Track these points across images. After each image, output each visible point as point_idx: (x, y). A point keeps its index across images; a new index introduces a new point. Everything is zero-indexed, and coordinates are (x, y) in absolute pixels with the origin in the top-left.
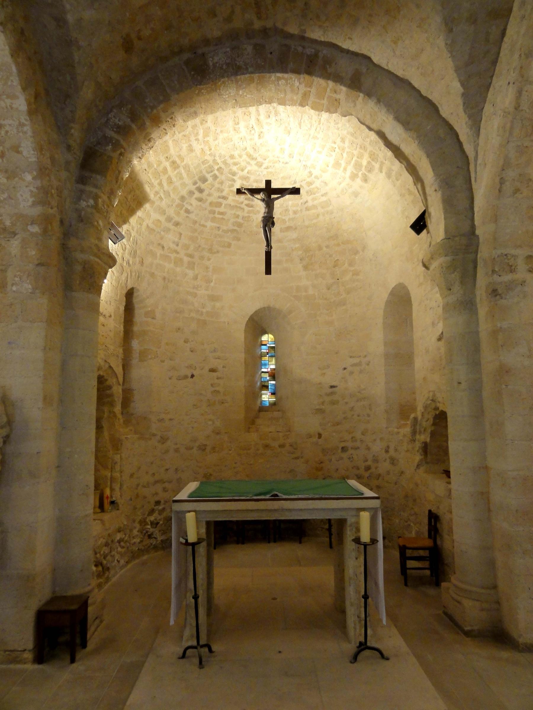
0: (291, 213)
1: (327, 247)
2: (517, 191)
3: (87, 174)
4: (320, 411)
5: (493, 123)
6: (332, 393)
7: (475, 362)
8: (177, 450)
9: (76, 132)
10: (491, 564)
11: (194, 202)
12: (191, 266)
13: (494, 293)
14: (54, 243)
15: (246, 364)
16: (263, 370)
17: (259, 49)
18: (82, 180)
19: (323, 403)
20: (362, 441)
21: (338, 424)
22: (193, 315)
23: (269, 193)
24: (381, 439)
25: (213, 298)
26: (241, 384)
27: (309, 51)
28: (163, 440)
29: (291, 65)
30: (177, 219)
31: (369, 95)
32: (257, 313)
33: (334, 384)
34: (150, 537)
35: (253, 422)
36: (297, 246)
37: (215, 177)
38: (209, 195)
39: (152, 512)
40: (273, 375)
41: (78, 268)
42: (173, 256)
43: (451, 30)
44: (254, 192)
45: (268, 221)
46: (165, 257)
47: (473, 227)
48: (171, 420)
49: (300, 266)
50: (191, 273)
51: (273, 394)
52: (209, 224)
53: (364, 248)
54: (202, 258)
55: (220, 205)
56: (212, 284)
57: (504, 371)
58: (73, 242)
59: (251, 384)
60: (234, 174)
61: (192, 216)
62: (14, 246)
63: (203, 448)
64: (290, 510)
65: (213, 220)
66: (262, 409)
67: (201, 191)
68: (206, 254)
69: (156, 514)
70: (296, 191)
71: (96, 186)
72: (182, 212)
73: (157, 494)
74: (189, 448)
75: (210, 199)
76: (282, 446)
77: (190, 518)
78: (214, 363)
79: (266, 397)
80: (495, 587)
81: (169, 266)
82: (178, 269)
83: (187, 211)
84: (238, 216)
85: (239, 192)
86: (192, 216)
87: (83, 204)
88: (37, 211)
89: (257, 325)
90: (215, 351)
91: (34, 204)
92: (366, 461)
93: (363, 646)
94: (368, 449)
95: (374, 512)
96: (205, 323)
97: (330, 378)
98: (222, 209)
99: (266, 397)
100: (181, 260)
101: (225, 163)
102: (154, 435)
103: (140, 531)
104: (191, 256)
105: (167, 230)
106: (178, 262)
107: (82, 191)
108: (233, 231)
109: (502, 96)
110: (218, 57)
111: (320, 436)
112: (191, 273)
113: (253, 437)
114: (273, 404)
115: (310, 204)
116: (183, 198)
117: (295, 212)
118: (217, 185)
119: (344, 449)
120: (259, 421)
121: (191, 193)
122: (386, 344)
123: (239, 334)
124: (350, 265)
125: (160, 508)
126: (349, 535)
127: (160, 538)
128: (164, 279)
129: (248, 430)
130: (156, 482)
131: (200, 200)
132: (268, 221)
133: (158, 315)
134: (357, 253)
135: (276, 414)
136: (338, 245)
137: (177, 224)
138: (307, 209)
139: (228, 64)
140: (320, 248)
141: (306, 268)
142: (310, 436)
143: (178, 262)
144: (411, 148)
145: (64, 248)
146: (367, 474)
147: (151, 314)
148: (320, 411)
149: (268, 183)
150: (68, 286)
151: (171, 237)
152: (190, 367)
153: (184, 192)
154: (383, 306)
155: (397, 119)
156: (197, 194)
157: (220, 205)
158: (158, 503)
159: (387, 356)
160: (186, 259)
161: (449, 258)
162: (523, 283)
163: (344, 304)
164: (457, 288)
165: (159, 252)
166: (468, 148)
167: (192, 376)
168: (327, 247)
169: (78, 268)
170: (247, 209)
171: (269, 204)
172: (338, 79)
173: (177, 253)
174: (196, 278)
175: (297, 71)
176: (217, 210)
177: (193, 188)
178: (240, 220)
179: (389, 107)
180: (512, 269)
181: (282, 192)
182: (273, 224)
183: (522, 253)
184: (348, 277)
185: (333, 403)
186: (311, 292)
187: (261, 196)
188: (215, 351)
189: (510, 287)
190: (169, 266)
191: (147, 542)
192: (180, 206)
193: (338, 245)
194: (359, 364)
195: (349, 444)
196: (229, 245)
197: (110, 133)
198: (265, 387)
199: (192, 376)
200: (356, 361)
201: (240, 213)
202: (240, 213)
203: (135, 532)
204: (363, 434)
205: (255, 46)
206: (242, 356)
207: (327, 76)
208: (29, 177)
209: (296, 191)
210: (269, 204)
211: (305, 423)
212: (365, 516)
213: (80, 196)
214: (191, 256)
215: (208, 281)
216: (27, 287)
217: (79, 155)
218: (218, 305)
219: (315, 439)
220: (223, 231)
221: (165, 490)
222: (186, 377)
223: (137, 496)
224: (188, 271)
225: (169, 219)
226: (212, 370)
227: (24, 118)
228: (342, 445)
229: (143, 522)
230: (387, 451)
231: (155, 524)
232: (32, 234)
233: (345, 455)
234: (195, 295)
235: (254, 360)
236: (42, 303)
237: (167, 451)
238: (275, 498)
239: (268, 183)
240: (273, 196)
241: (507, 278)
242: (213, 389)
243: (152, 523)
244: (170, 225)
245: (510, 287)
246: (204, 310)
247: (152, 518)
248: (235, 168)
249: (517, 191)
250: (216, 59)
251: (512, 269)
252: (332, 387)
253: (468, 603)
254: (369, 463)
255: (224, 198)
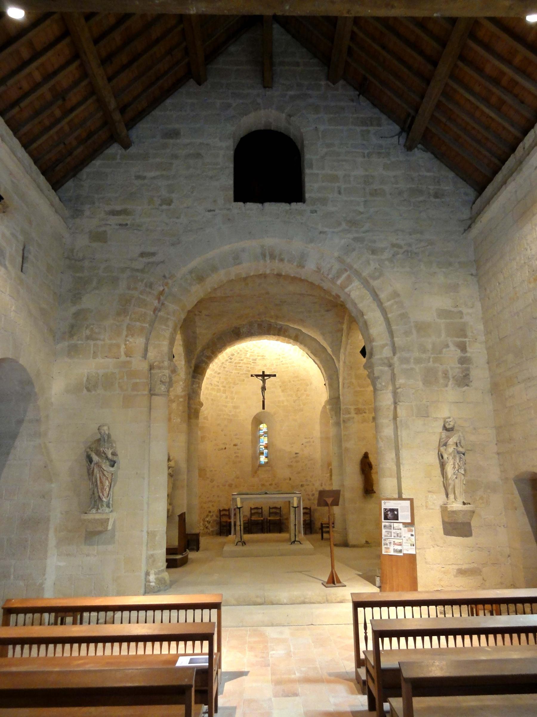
0: (275, 365)
1: (293, 381)
2: (349, 387)
3: (196, 375)
4: (290, 466)
5: (341, 363)
6: (296, 457)
7: (340, 446)
8: (218, 486)
9: (193, 362)
10: (345, 521)
11: (228, 364)
12: (224, 392)
13: (344, 421)
14: (187, 402)
15: (252, 442)
16: (261, 444)
17: (260, 326)
18: (194, 377)
19: (292, 462)
20: (310, 481)
21: (299, 473)
22: (225, 417)
23: (263, 376)
24: (319, 480)
25: (235, 407)
26: (250, 452)
27: (279, 327)
28: (212, 481)
29: (272, 332)
30: (219, 371)
31: (301, 343)
32: (257, 414)
33: (297, 452)
34: (207, 528)
35: (256, 472)
36: (278, 380)
37: (239, 353)
38: (235, 360)
39: (207, 516)
40: (266, 447)
41: (193, 411)
42: (216, 388)
43: (324, 335)
44: (257, 376)
45: (264, 389)
46: (213, 389)
47: (339, 395)
48: (215, 471)
49: (280, 390)
50: (224, 395)
51: (266, 457)
52: (234, 371)
53: (311, 384)
54: (230, 387)
55: (240, 363)
56: (235, 400)
57: (347, 450)
58: (192, 402)
59: (254, 452)
60: (247, 351)
61: (226, 369)
62: (174, 405)
63: (230, 486)
64: (271, 498)
65: (236, 369)
66: (261, 465)
67: (231, 359)
68: (232, 385)
69: (209, 517)
70: (275, 376)
71: (199, 379)
72: (222, 369)
73: (209, 507)
74: (224, 486)
75: (236, 361)
76: (271, 485)
77: (238, 500)
78: (236, 441)
79: (263, 459)
80: (346, 529)
81: (214, 393)
82: (218, 394)
83: (224, 368)
84: (248, 367)
85: (252, 376)
86: (226, 369)
87: (194, 386)
88: (183, 393)
89: (257, 421)
90: (236, 435)
91: (182, 391)
92: (312, 491)
93: (295, 541)
94: (313, 485)
95: (299, 499)
96: (230, 421)
97: (295, 449)
98: (240, 365)
99: (263, 459)
100: (220, 389)
101: (243, 348)
102: (208, 478)
103: (203, 525)
104: (224, 387)
105: (215, 377)
106: (219, 390)
107: (194, 381)
108: (245, 374)
109: (342, 357)
110: (244, 330)
111: (290, 479)
112: (224, 395)
113: (255, 480)
114: (266, 463)
115: (284, 362)
116: (223, 363)
117: (277, 365)
118: (239, 355)
119: (302, 486)
120: (259, 472)
121: (227, 360)
122: (321, 433)
123: (249, 427)
124: (305, 391)
125: (211, 514)
126: (291, 505)
127: (211, 529)
128: (212, 400)
129: (253, 476)
130: (210, 501)
131: (230, 362)
132: (264, 389)
133: (209, 418)
134: (307, 385)
135: (268, 468)
136: (299, 381)
137: (219, 373)
138: (283, 364)
139: (248, 332)
140: (290, 382)
141: (283, 391)
142: (285, 479)
143: (219, 390)
144: (318, 362)
145: (189, 403)
146: (312, 498)
147: (206, 418)
148: (290, 466)
149: (263, 372)
150: (189, 418)
151: (216, 379)
152: (224, 444)
153: (224, 361)
154: (319, 413)
155: (312, 353)
156: (229, 360)
157: (240, 363)
158: (210, 512)
159: (321, 438)
160: (222, 389)
161: (331, 406)
162: (353, 418)
163: (302, 411)
164: (334, 417)
165: (210, 387)
166: (337, 365)
167: (225, 448)
168: (293, 381)
169: (193, 411)
170: (253, 364)
171: (264, 381)
172: (289, 337)
173: (218, 386)
174: (227, 398)
175: (274, 335)
176: (238, 365)
177: (228, 358)
178: (249, 369)
179: (309, 348)
180: (349, 413)
181: (269, 376)
182: (265, 389)
183: (352, 408)
184: (304, 397)
185: (297, 462)
186: (285, 404)
187: (260, 378)
188: (236, 435)
189: (349, 419)
190: (214, 393)
191: (206, 530)
192: (221, 366)
193: (299, 381)
194: (310, 442)
195: (304, 483)
196: (244, 380)
197: (204, 359)
198: (262, 453)
199: (225, 448)
200: (308, 440)
201: (249, 366)
202: (249, 366)
203: (201, 524)
204: (311, 478)
205: (258, 324)
206: (250, 437)
207: (286, 336)
208: (181, 383)
209: (275, 376)
210: (264, 381)
211: (283, 472)
212: (295, 499)
213: (193, 383)
214: (224, 387)
215: (233, 398)
216: (179, 420)
217: (193, 368)
218: (238, 410)
219: (288, 481)
220: (241, 374)
221: (213, 506)
222: (222, 449)
223: (202, 507)
224: (223, 395)
225: (216, 372)
226: (235, 445)
227: (183, 366)
228: (301, 483)
229: (204, 520)
230: (322, 486)
231: (209, 522)
232: (181, 402)
233: (302, 489)
234: (226, 406)
235: (256, 439)
236: (184, 426)
237: (213, 487)
238: (266, 493)
239: (263, 372)
240: (265, 378)
241: (349, 416)
242: (235, 455)
243: (207, 522)
244: (216, 375)
245: (349, 419)
246: (231, 414)
247: (207, 519)
248: (247, 349)
249: (349, 387)
250: (244, 330)
251: (349, 413)
252: (296, 453)
253: (335, 535)
254: (314, 492)
255: (242, 360)
